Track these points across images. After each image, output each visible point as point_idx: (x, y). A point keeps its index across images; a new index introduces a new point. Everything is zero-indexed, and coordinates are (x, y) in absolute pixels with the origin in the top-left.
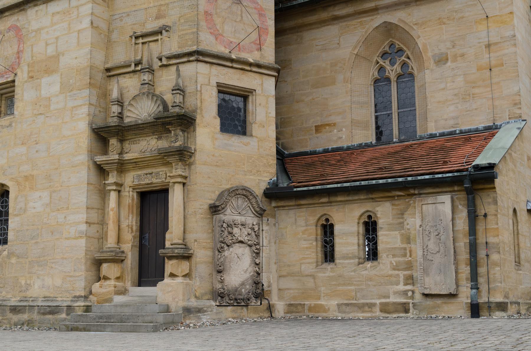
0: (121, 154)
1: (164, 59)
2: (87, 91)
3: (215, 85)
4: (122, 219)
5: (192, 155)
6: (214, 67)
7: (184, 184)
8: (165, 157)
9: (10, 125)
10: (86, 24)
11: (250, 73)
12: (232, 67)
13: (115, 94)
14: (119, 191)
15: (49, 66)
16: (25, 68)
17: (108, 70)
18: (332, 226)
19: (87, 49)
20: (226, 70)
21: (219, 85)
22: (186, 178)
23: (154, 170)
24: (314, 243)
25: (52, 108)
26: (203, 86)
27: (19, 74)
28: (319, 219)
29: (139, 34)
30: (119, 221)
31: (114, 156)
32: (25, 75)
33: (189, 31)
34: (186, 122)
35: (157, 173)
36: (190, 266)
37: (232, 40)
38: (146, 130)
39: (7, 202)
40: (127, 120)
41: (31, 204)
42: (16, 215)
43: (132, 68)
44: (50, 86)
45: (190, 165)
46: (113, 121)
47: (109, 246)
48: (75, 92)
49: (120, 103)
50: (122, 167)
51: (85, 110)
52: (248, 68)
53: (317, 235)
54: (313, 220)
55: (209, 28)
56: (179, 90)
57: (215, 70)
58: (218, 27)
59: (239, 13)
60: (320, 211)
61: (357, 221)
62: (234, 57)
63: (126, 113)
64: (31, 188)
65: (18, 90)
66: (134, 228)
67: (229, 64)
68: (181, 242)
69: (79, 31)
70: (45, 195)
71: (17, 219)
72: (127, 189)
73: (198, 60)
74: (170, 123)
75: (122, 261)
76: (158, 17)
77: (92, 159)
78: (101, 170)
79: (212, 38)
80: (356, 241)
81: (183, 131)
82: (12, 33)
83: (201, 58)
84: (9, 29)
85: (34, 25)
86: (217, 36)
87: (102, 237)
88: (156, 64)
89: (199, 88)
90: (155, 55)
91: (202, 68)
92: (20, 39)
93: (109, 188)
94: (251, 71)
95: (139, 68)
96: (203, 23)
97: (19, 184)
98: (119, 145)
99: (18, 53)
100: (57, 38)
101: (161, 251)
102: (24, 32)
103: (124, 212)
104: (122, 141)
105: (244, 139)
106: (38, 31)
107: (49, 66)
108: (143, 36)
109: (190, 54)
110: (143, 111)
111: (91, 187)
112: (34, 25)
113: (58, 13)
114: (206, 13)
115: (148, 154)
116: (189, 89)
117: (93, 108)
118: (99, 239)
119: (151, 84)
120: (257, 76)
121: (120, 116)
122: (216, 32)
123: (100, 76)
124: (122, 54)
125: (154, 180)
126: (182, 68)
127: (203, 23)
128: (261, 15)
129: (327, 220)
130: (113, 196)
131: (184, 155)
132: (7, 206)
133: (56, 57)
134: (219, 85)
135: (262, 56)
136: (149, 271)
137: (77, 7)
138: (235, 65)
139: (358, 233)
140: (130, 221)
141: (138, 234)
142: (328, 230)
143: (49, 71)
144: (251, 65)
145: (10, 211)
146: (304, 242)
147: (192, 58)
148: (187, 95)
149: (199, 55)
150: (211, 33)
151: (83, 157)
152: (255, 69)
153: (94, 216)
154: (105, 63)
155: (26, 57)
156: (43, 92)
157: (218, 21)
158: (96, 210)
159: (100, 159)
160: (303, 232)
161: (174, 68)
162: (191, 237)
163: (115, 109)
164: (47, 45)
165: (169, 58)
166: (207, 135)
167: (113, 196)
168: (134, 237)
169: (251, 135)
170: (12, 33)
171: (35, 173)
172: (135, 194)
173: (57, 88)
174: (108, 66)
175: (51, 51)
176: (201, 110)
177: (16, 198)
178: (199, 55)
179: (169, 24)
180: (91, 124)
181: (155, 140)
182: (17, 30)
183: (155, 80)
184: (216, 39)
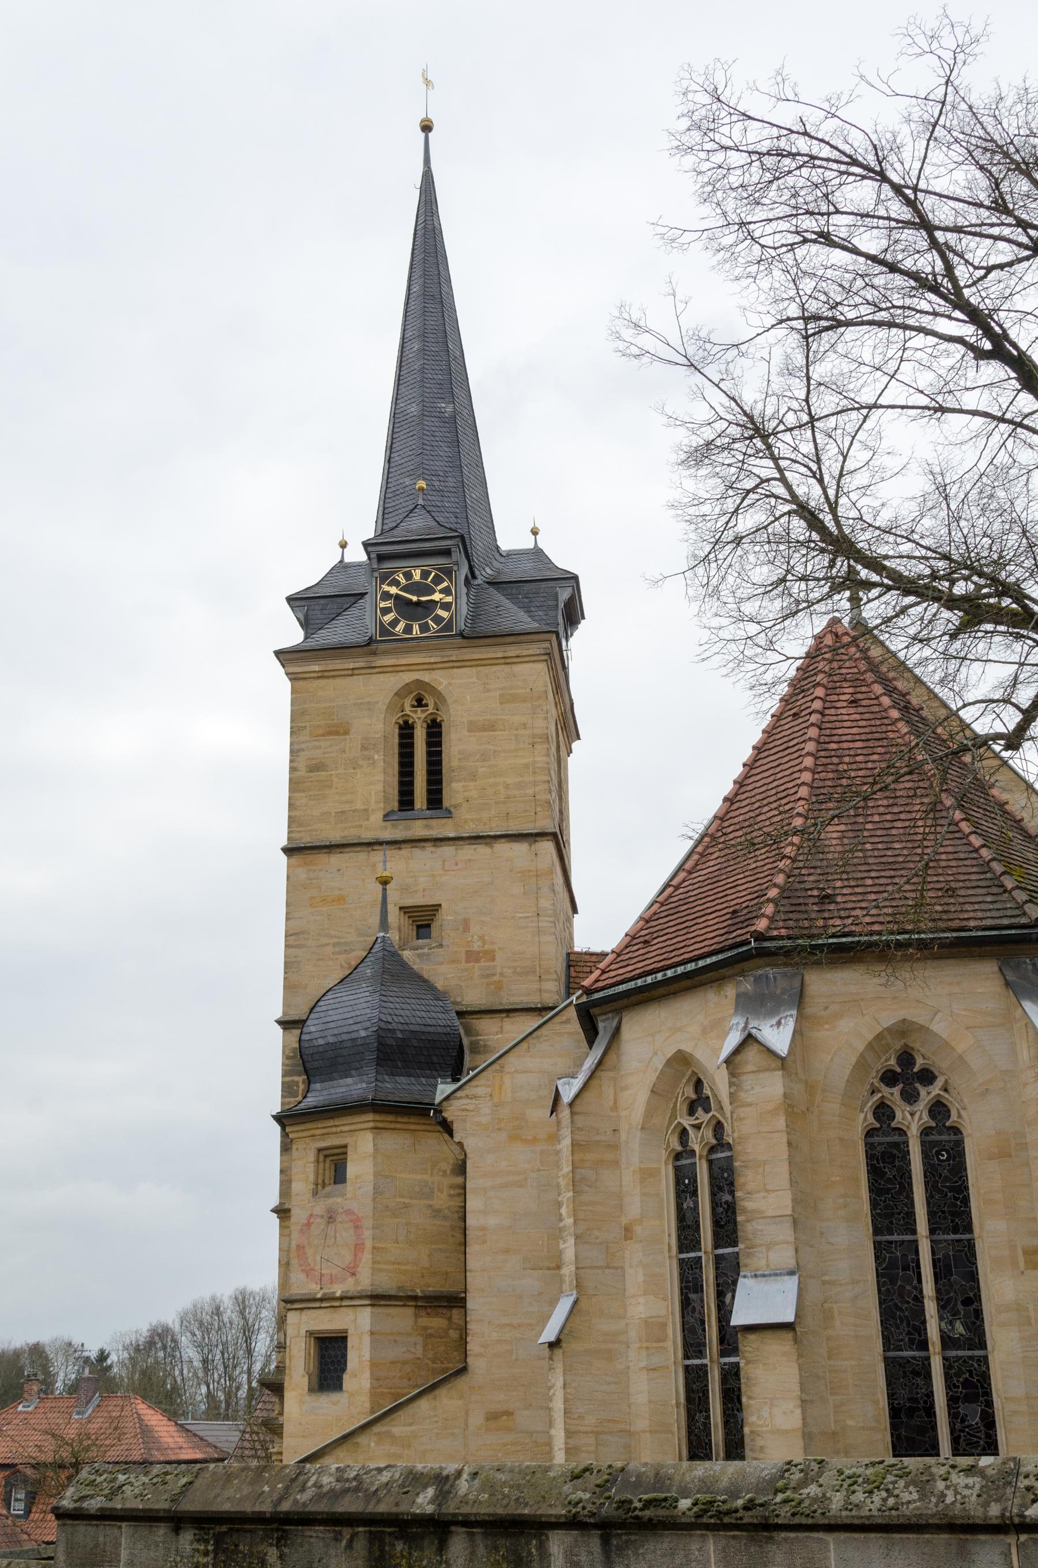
12: (320, 1308)
20: (317, 1312)
21: (310, 1333)
55: (301, 1265)
58: (310, 1261)
67: (317, 1305)
79: (302, 1277)
86: (308, 1272)
94: (341, 1306)
96: (294, 1262)
105: (335, 1396)
114: (298, 1246)
120: (350, 1311)
128: (357, 1227)
135: (357, 1283)
150: (303, 1271)
157: (309, 1252)
176: (290, 1369)
184: (308, 1276)
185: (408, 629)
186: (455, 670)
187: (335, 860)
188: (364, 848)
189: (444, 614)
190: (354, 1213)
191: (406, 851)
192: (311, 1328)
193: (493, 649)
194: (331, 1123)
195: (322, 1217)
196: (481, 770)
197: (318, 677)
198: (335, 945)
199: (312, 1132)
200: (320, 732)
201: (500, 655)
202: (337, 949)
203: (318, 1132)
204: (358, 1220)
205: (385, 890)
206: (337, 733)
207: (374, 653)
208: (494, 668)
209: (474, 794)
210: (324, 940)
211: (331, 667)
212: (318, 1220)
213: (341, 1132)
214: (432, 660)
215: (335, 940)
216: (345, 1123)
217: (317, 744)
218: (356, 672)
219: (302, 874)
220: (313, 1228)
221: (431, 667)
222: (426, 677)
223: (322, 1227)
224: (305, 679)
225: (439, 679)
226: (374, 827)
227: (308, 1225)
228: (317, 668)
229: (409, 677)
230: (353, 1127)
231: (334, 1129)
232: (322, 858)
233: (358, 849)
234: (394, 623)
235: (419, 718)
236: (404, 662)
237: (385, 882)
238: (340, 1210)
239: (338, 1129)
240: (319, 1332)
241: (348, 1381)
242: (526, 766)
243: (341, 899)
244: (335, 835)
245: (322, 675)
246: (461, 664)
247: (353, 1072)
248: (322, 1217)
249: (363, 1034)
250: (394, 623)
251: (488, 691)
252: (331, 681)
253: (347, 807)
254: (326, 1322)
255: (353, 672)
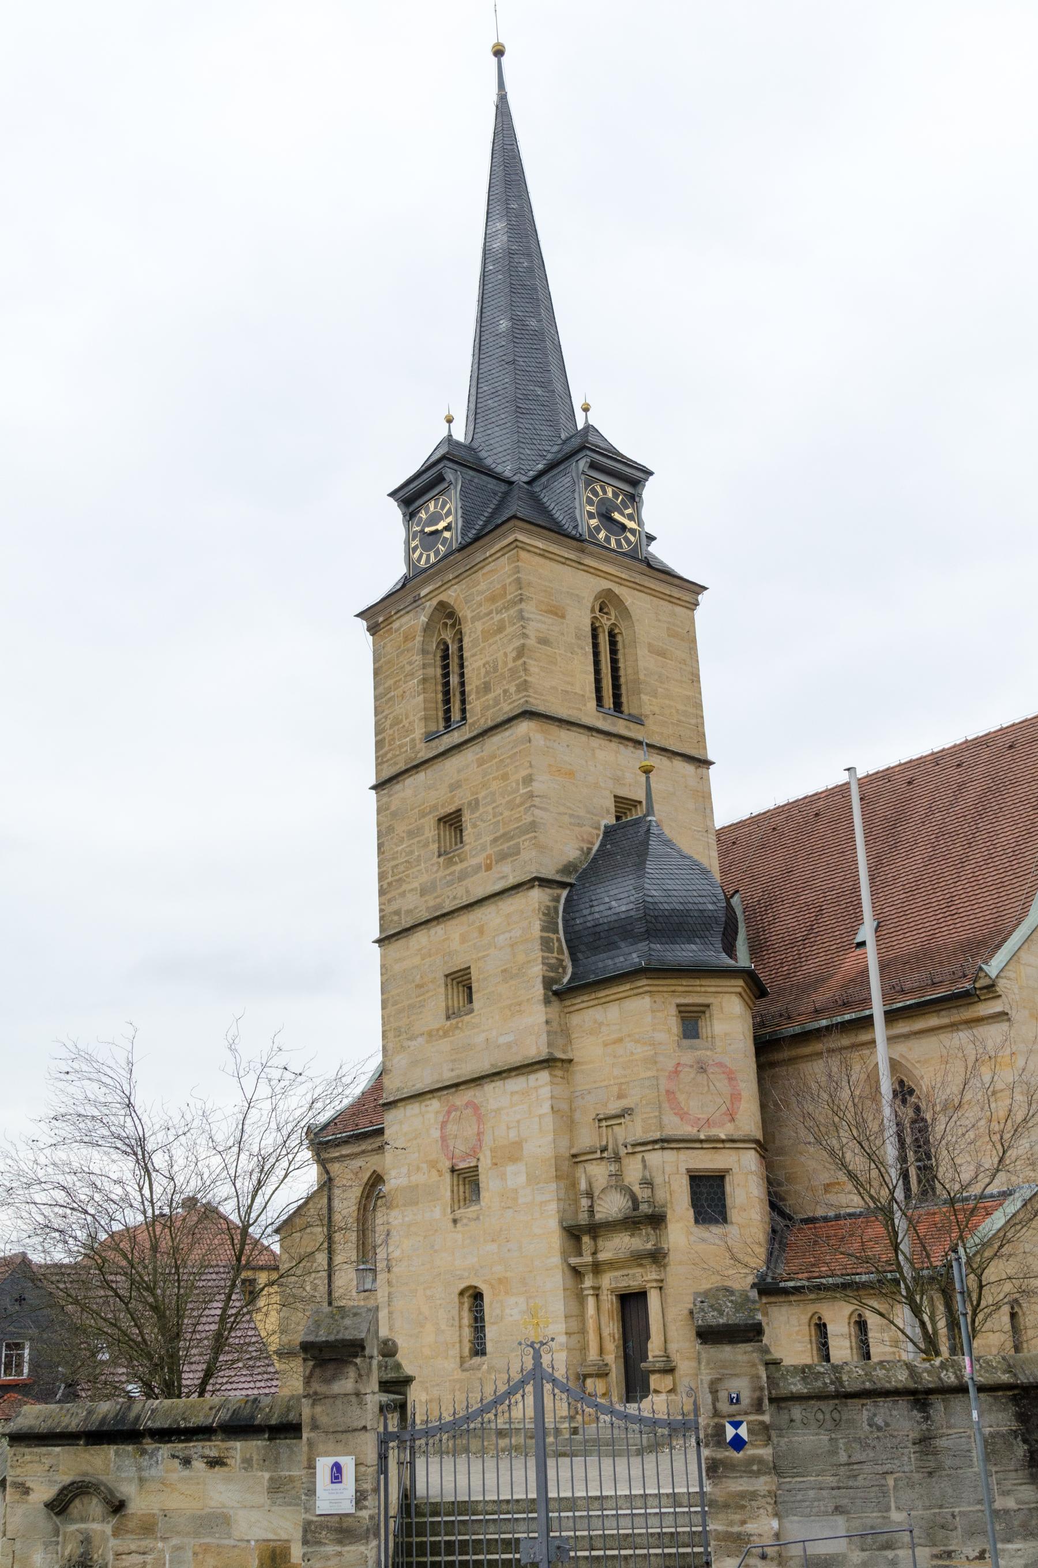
0: (594, 1253)
1: (629, 1147)
2: (554, 1185)
3: (685, 1171)
4: (603, 1327)
5: (665, 1255)
6: (682, 1151)
7: (661, 1288)
8: (638, 1258)
9: (478, 1218)
10: (546, 1108)
11: (724, 1151)
13: (583, 1186)
14: (597, 1295)
15: (512, 1153)
16: (488, 1153)
17: (574, 1156)
18: (825, 1325)
19: (550, 1137)
20: (696, 1151)
21: (688, 1171)
22: (662, 1281)
23: (631, 1272)
24: (809, 1346)
25: (520, 1201)
26: (671, 1176)
27: (482, 1158)
28: (811, 1318)
29: (601, 1116)
30: (600, 1329)
31: (588, 1259)
32: (489, 1161)
33: (652, 1115)
34: (657, 1220)
35: (634, 1275)
36: (674, 1380)
37: (699, 1116)
38: (618, 1227)
39: (481, 1306)
40: (598, 1216)
41: (508, 1311)
42: (493, 1323)
43: (598, 1155)
44: (516, 1176)
45: (665, 1266)
46: (583, 1218)
47: (591, 1358)
48: (541, 1185)
49: (590, 1195)
50: (597, 1268)
51: (553, 1207)
52: (721, 1145)
53: (811, 1336)
54: (805, 1319)
55: (672, 1109)
56: (648, 1183)
57: (683, 1155)
59: (705, 1083)
60: (812, 1308)
61: (847, 1321)
62: (702, 1137)
63: (596, 1208)
64: (507, 1293)
65: (482, 1178)
66: (616, 1336)
68: (662, 1353)
69: (540, 1116)
70: (521, 1300)
71: (495, 1327)
72: (605, 1292)
73: (663, 1149)
74: (639, 1223)
75: (607, 1374)
76: (620, 1096)
77: (566, 1261)
78: (577, 1273)
79: (676, 1119)
80: (848, 1344)
81: (654, 1229)
82: (469, 1111)
83: (666, 1145)
84: (468, 1105)
85: (493, 1105)
86: (683, 1115)
87: (584, 1348)
88: (623, 1151)
89: (667, 1180)
90: (621, 1141)
91: (669, 1156)
92: (480, 1119)
93: (586, 1292)
95: (605, 1155)
96: (666, 1105)
97: (492, 1287)
98: (593, 1243)
99: (478, 1134)
100: (518, 1122)
101: (643, 1365)
102: (483, 1110)
103: (604, 1319)
104: (594, 1238)
106: (498, 1111)
107: (512, 1153)
108: (606, 1119)
109: (655, 1142)
110: (612, 1206)
111: (568, 1293)
112: (493, 1105)
113: (517, 1092)
114: (667, 1091)
115: (621, 1256)
116: (658, 1180)
117: (562, 1203)
118: (581, 1350)
119: (618, 1175)
121: (591, 1211)
122: (681, 1112)
123: (565, 1166)
124: (587, 1138)
125: (632, 1283)
126: (648, 1156)
127: (666, 1105)
128: (730, 1079)
129: (820, 1318)
130: (591, 1302)
131: (657, 1257)
132: (482, 1310)
133: (518, 1145)
134: (688, 1171)
136: (635, 1385)
137: (536, 1088)
138: (705, 1146)
139: (850, 1335)
140: (612, 1328)
141: (621, 1342)
142: (821, 1328)
143: (514, 1159)
144: (723, 1141)
145: (486, 1318)
146: (799, 1345)
147: (657, 1147)
148: (656, 1187)
149: (665, 1143)
151: (556, 1260)
152: (727, 1145)
153: (574, 1325)
154: (571, 1147)
155: (488, 1140)
156: (509, 1183)
157: (681, 1098)
158: (574, 1318)
159: (574, 1261)
160: (797, 1333)
161: (639, 1156)
162: (673, 1347)
163: (585, 1202)
164: (508, 1128)
165: (634, 1145)
166: (681, 1231)
167: (591, 1302)
168: (617, 1347)
169: (732, 1223)
170: (469, 1111)
171: (508, 1274)
172: (614, 1298)
173: (522, 1179)
174: (574, 1151)
175: (513, 1135)
176: (672, 1203)
177: (491, 1303)
178: (665, 1143)
179: (632, 1106)
180: (561, 1222)
181: (628, 1238)
182: (476, 1108)
183: (623, 1169)
184: (682, 1119)
185: (607, 539)
186: (636, 592)
187: (566, 735)
188: (586, 732)
189: (632, 538)
190: (726, 1066)
191: (614, 745)
192: (693, 1165)
193: (663, 585)
194: (698, 982)
195: (691, 1066)
196: (660, 690)
197: (540, 555)
198: (571, 816)
199: (673, 988)
200: (543, 608)
201: (668, 593)
202: (572, 821)
203: (680, 989)
204: (731, 1072)
205: (648, 778)
206: (556, 614)
207: (582, 551)
208: (662, 602)
209: (656, 710)
210: (562, 809)
211: (551, 549)
212: (687, 1069)
213: (705, 992)
214: (623, 576)
215: (571, 812)
216: (711, 985)
217: (543, 619)
218: (568, 562)
219: (702, 752)
220: (682, 1075)
221: (621, 582)
222: (617, 590)
223: (692, 1076)
224: (529, 551)
225: (630, 598)
226: (589, 713)
227: (676, 1072)
228: (541, 545)
229: (606, 585)
230: (719, 989)
231: (698, 989)
232: (553, 729)
233: (582, 731)
234: (598, 529)
235: (606, 623)
236: (604, 568)
237: (647, 771)
238: (711, 1062)
239: (703, 989)
240: (698, 1170)
241: (733, 1214)
242: (688, 698)
243: (571, 774)
244: (563, 713)
245: (544, 554)
246: (641, 588)
247: (697, 940)
248: (691, 1066)
249: (711, 907)
250: (598, 529)
251: (659, 621)
252: (547, 562)
253: (569, 688)
254: (706, 1161)
255: (565, 562)
